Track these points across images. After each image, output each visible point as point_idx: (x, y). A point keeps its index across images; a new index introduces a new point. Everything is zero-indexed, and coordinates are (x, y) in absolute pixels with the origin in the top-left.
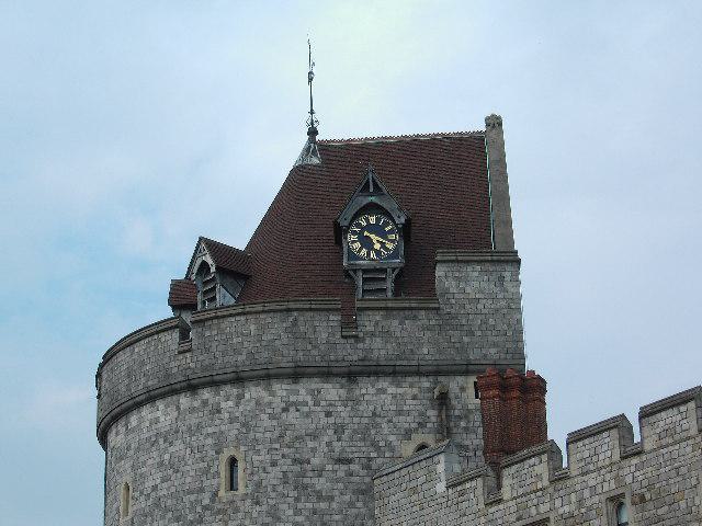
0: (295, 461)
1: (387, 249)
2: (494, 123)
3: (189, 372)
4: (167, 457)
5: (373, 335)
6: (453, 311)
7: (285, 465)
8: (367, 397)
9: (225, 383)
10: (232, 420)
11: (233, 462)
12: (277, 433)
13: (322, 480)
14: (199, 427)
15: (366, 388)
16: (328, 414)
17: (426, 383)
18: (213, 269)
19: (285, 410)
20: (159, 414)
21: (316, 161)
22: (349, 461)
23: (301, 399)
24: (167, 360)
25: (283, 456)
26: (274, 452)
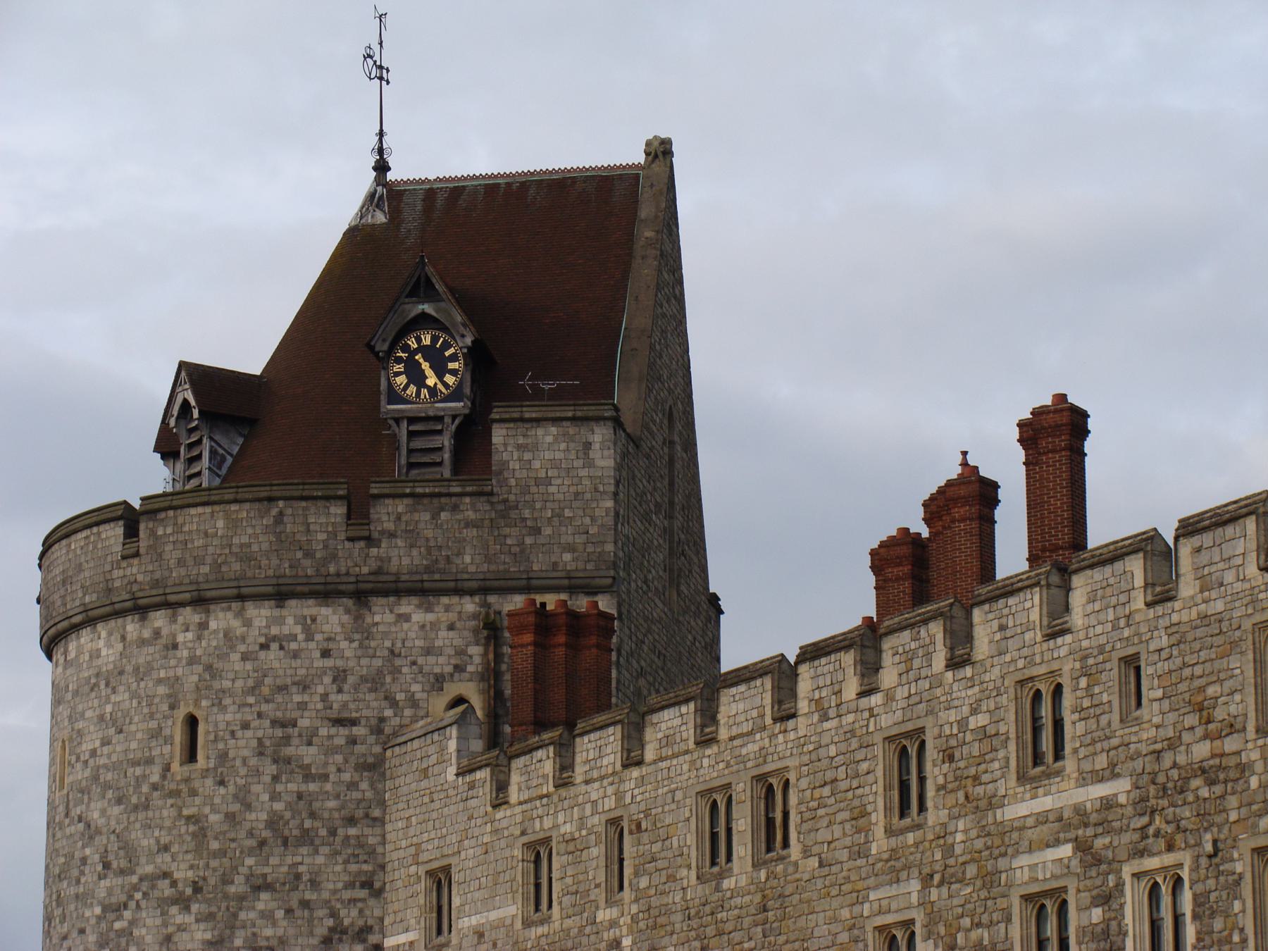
0: (275, 723)
1: (446, 385)
2: (661, 151)
3: (135, 588)
4: (109, 708)
5: (392, 535)
6: (512, 497)
7: (263, 729)
8: (381, 628)
9: (182, 604)
10: (192, 661)
11: (192, 722)
12: (250, 683)
13: (313, 750)
14: (150, 668)
15: (381, 614)
16: (326, 654)
17: (469, 605)
18: (196, 413)
19: (265, 647)
20: (101, 643)
21: (381, 218)
22: (353, 722)
23: (286, 630)
24: (108, 568)
25: (260, 715)
26: (247, 709)
